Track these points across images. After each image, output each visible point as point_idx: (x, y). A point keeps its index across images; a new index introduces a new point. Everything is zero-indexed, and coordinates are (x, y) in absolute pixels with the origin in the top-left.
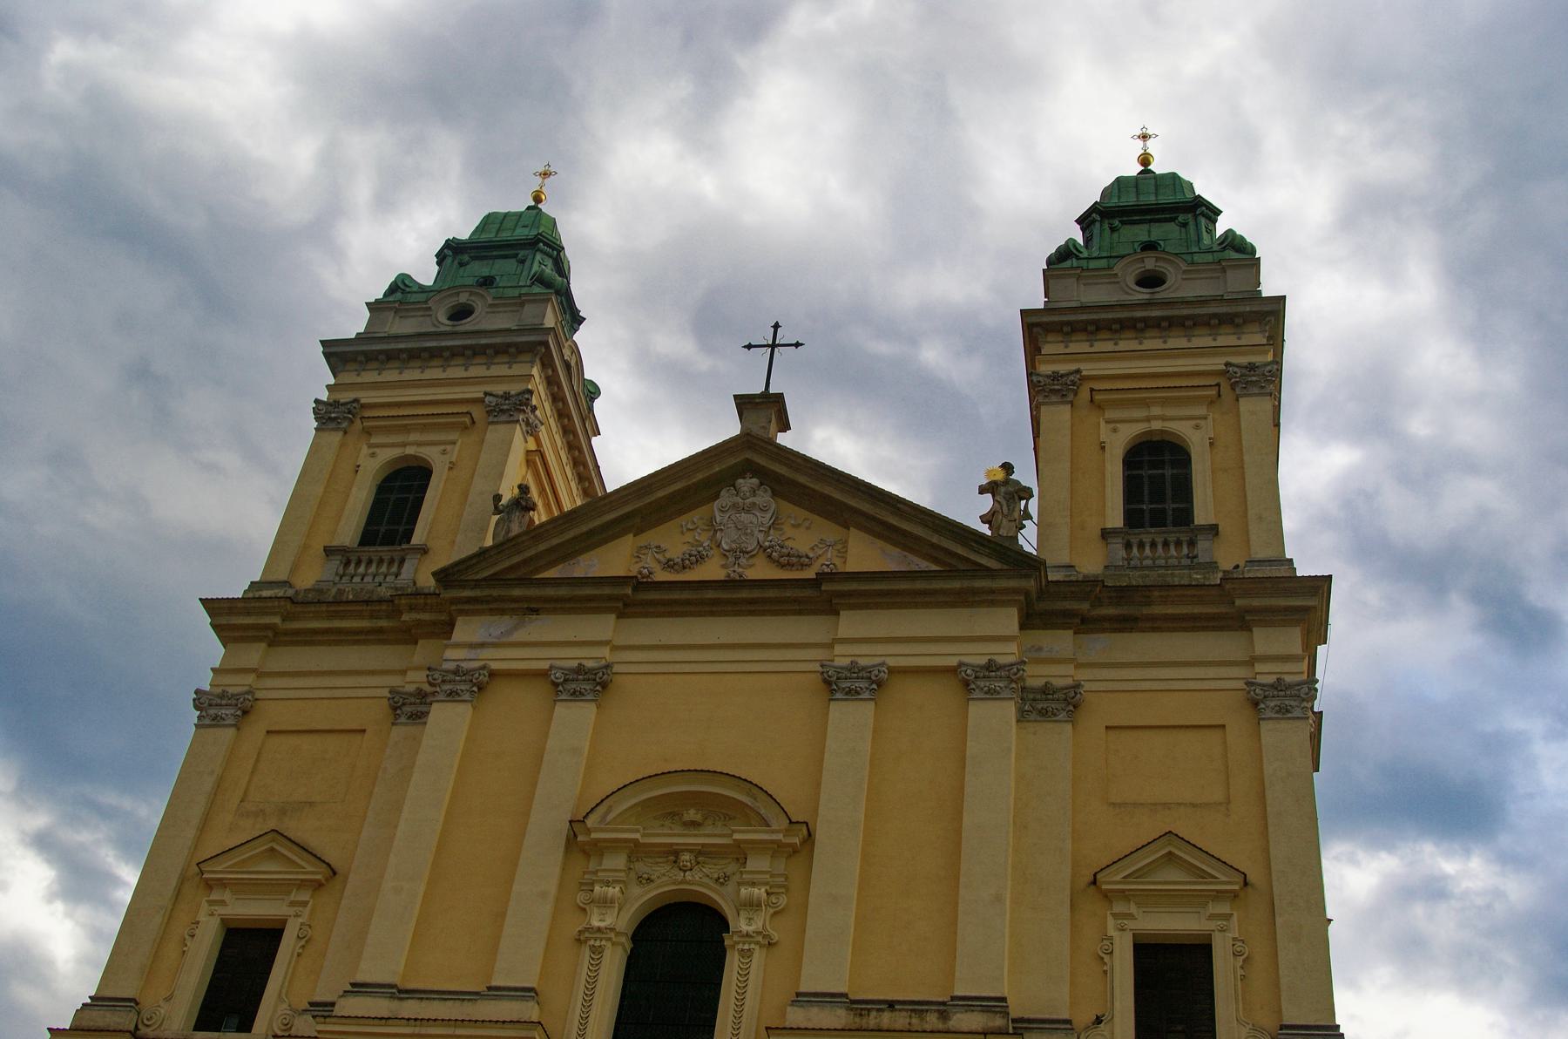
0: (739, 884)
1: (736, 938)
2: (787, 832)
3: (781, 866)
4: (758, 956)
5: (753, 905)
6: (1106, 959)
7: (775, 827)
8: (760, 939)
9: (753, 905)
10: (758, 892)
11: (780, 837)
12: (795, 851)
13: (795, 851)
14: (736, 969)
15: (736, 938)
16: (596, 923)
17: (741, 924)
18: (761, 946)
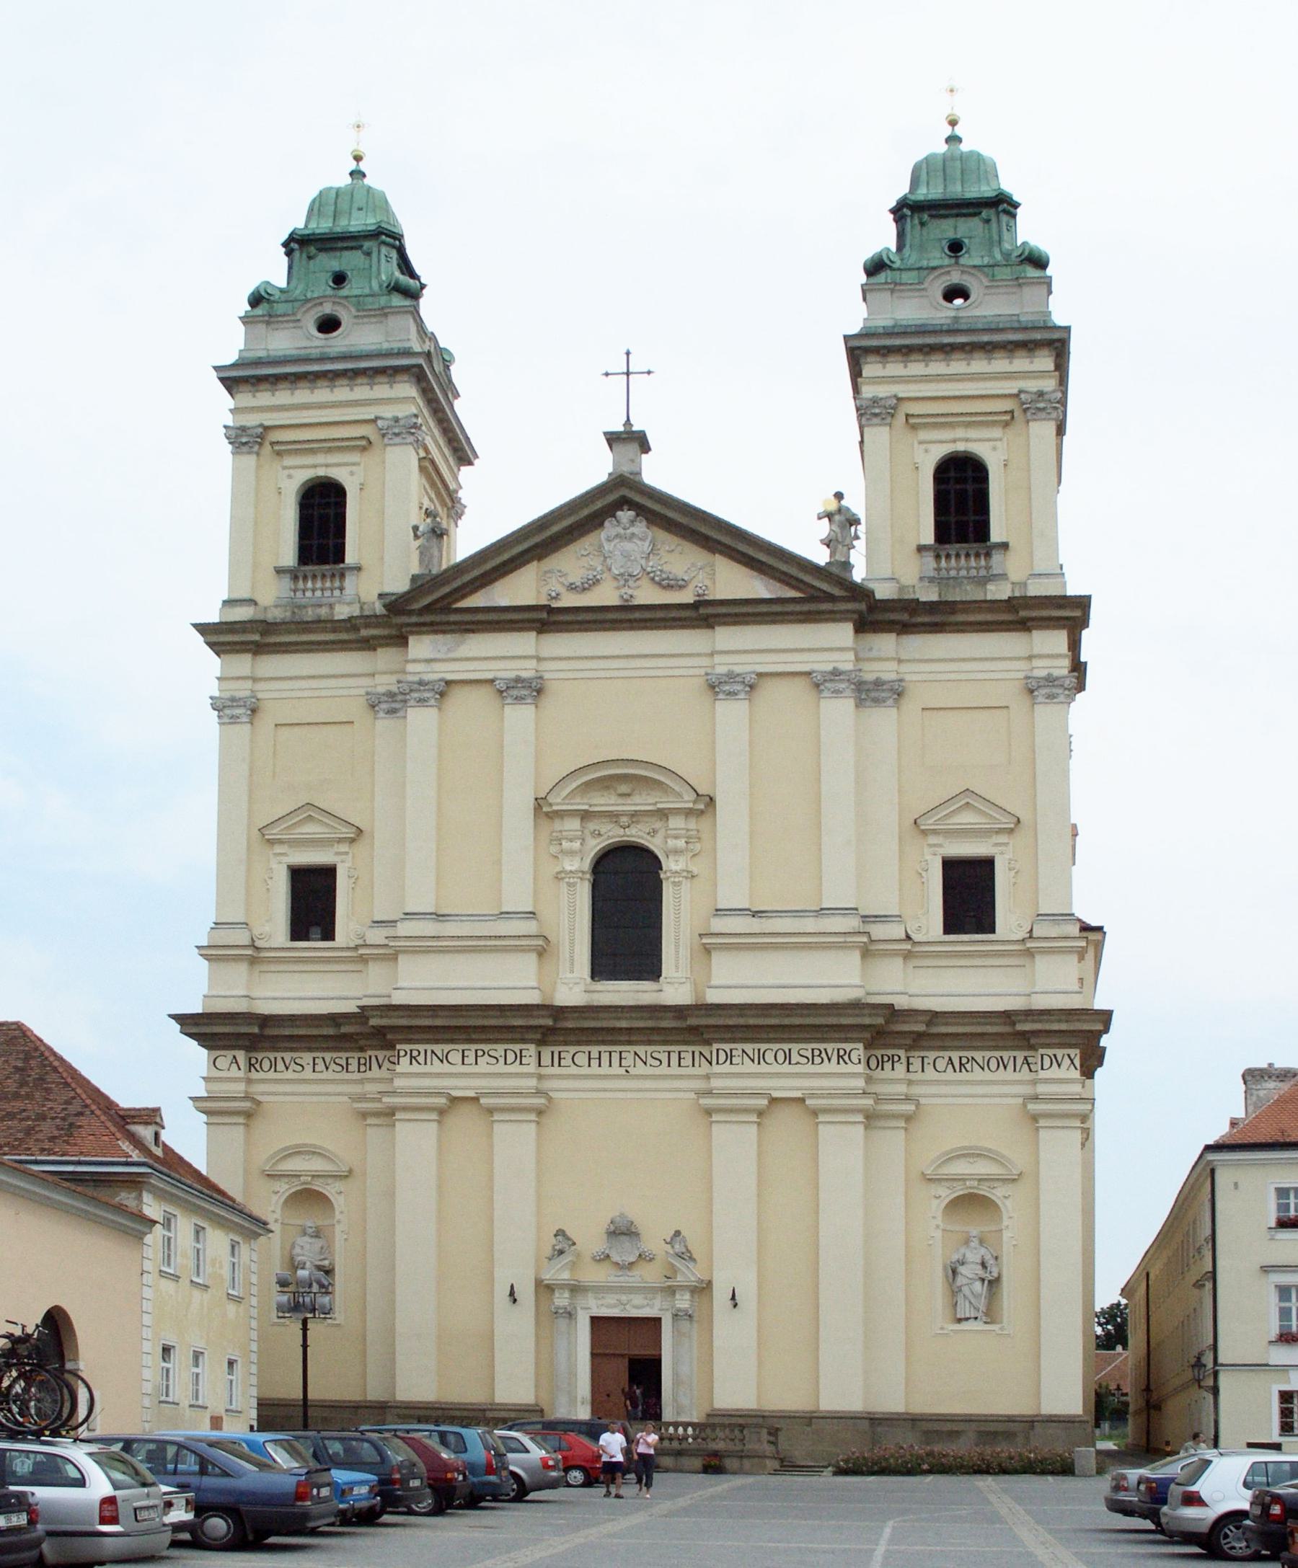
0: (666, 837)
1: (668, 874)
2: (695, 802)
3: (692, 824)
4: (686, 885)
5: (677, 852)
6: (924, 874)
7: (686, 798)
8: (685, 874)
9: (677, 852)
10: (681, 843)
11: (691, 805)
12: (702, 812)
13: (702, 812)
14: (671, 894)
15: (668, 874)
16: (568, 868)
17: (670, 865)
18: (686, 878)
